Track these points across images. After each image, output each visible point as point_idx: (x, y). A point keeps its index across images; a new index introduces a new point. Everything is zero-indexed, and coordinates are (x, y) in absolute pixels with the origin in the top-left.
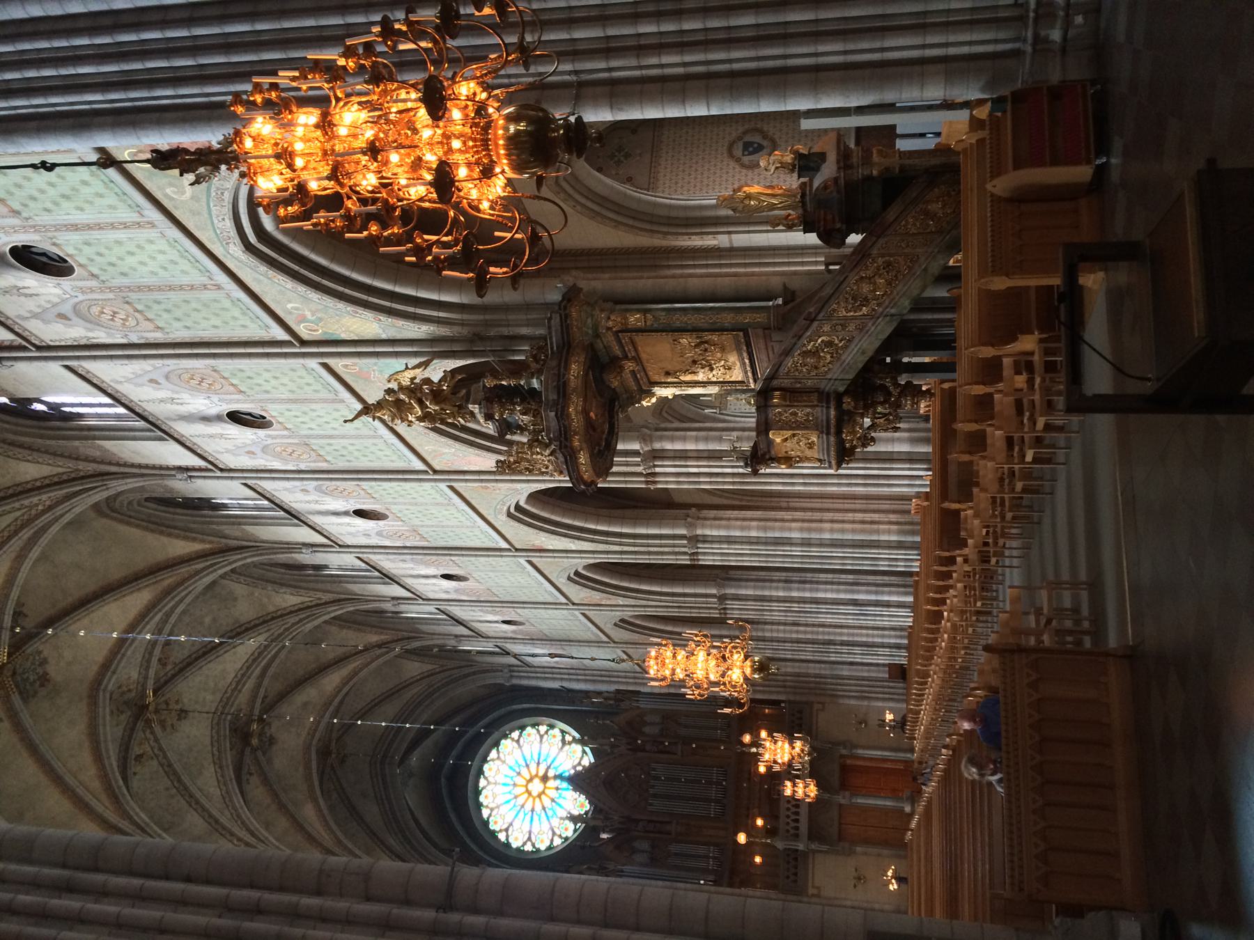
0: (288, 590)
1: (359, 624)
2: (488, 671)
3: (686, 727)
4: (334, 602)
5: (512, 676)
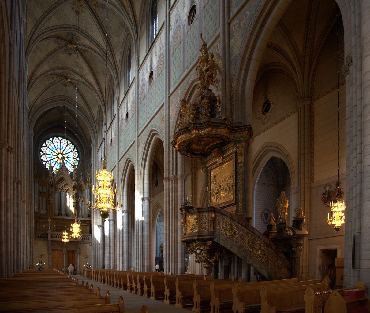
1: (109, 89)
2: (95, 137)
3: (82, 204)
4: (117, 76)
5: (94, 146)
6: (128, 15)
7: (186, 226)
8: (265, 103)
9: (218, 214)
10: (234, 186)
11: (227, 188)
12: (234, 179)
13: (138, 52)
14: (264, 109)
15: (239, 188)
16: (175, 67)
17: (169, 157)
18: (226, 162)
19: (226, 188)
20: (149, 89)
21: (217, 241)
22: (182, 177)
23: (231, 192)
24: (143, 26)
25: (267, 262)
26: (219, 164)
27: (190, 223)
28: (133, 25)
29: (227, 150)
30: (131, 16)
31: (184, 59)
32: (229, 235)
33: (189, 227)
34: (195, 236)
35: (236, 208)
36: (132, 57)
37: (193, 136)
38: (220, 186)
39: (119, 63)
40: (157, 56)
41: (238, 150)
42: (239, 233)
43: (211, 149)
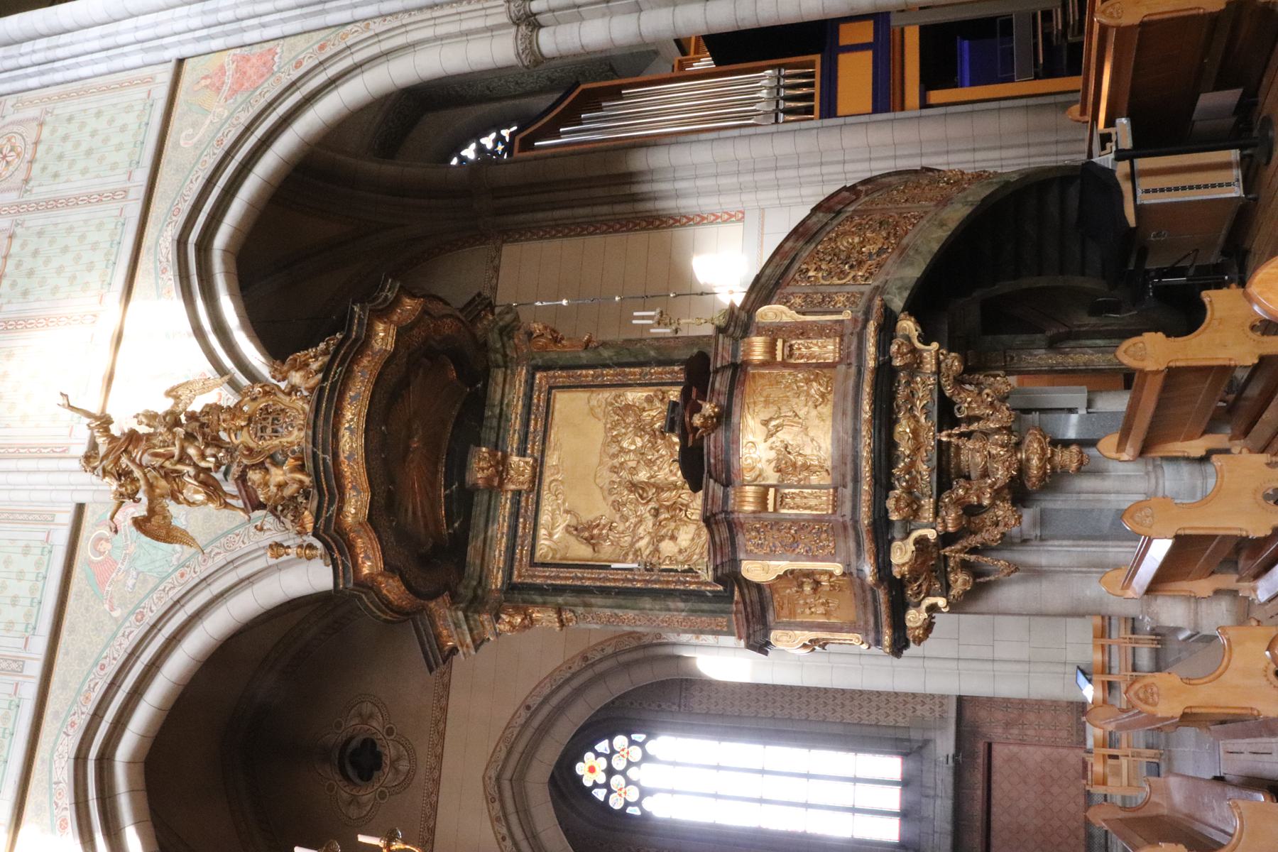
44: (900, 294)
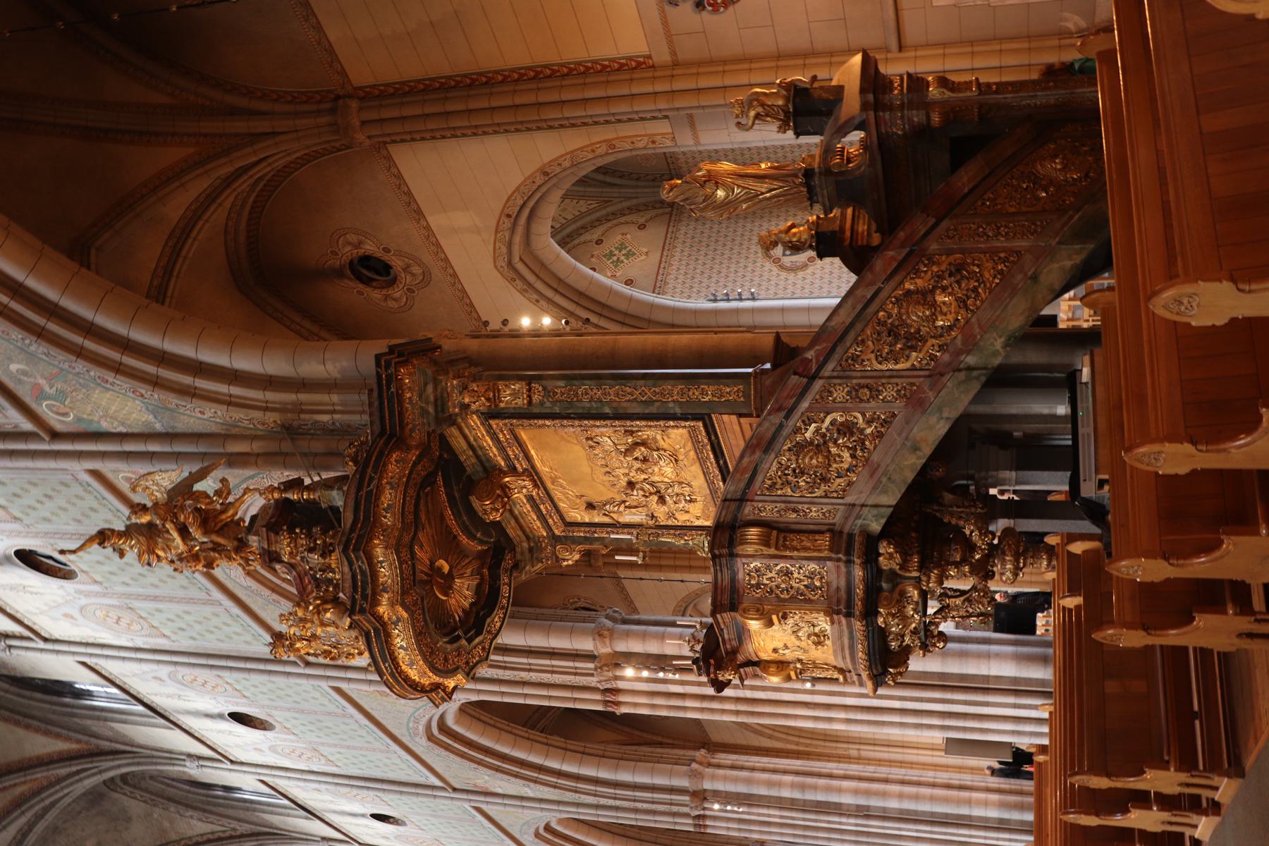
0: (196, 814)
6: (60, 780)
7: (799, 666)
8: (361, 279)
9: (748, 509)
10: (628, 423)
11: (637, 454)
12: (598, 423)
13: (172, 756)
14: (378, 278)
15: (635, 399)
16: (208, 636)
17: (524, 683)
18: (528, 457)
19: (636, 459)
20: (287, 734)
21: (877, 517)
22: (606, 633)
23: (656, 441)
24: (94, 729)
25: (1002, 255)
26: (536, 486)
27: (786, 647)
28: (90, 765)
29: (480, 453)
30: (63, 771)
31: (180, 601)
32: (853, 456)
33: (805, 651)
34: (850, 627)
35: (725, 417)
36: (190, 776)
37: (405, 615)
38: (631, 485)
39: (211, 823)
40: (180, 693)
41: (473, 407)
42: (845, 411)
43: (475, 522)
44: (876, 520)
